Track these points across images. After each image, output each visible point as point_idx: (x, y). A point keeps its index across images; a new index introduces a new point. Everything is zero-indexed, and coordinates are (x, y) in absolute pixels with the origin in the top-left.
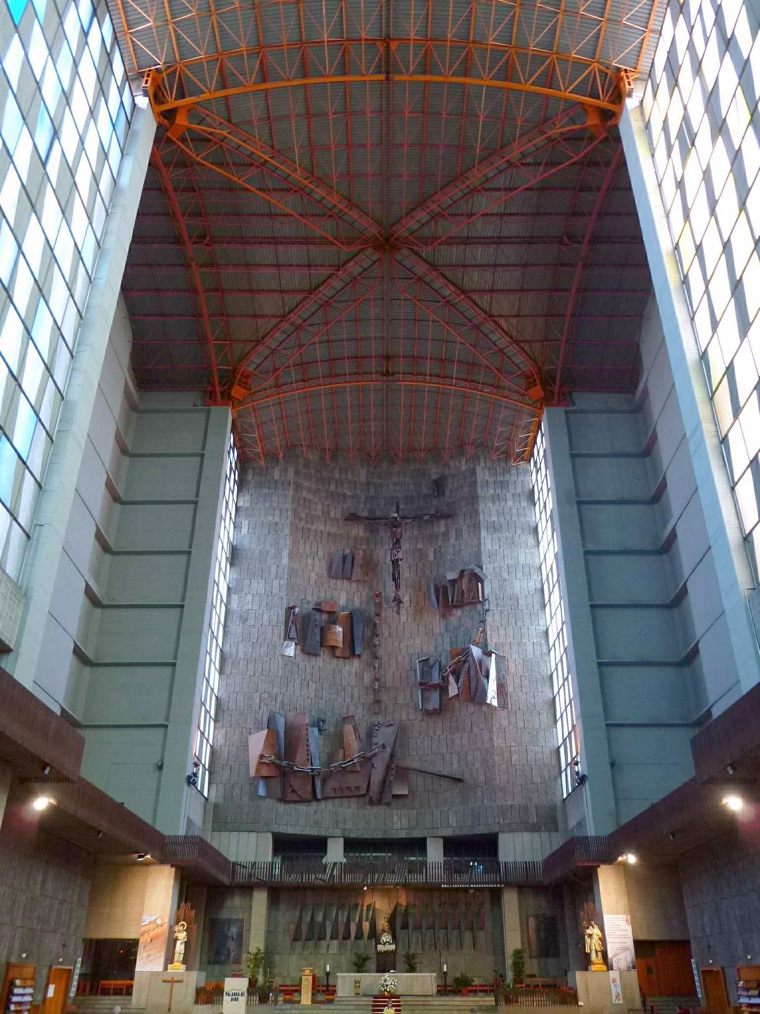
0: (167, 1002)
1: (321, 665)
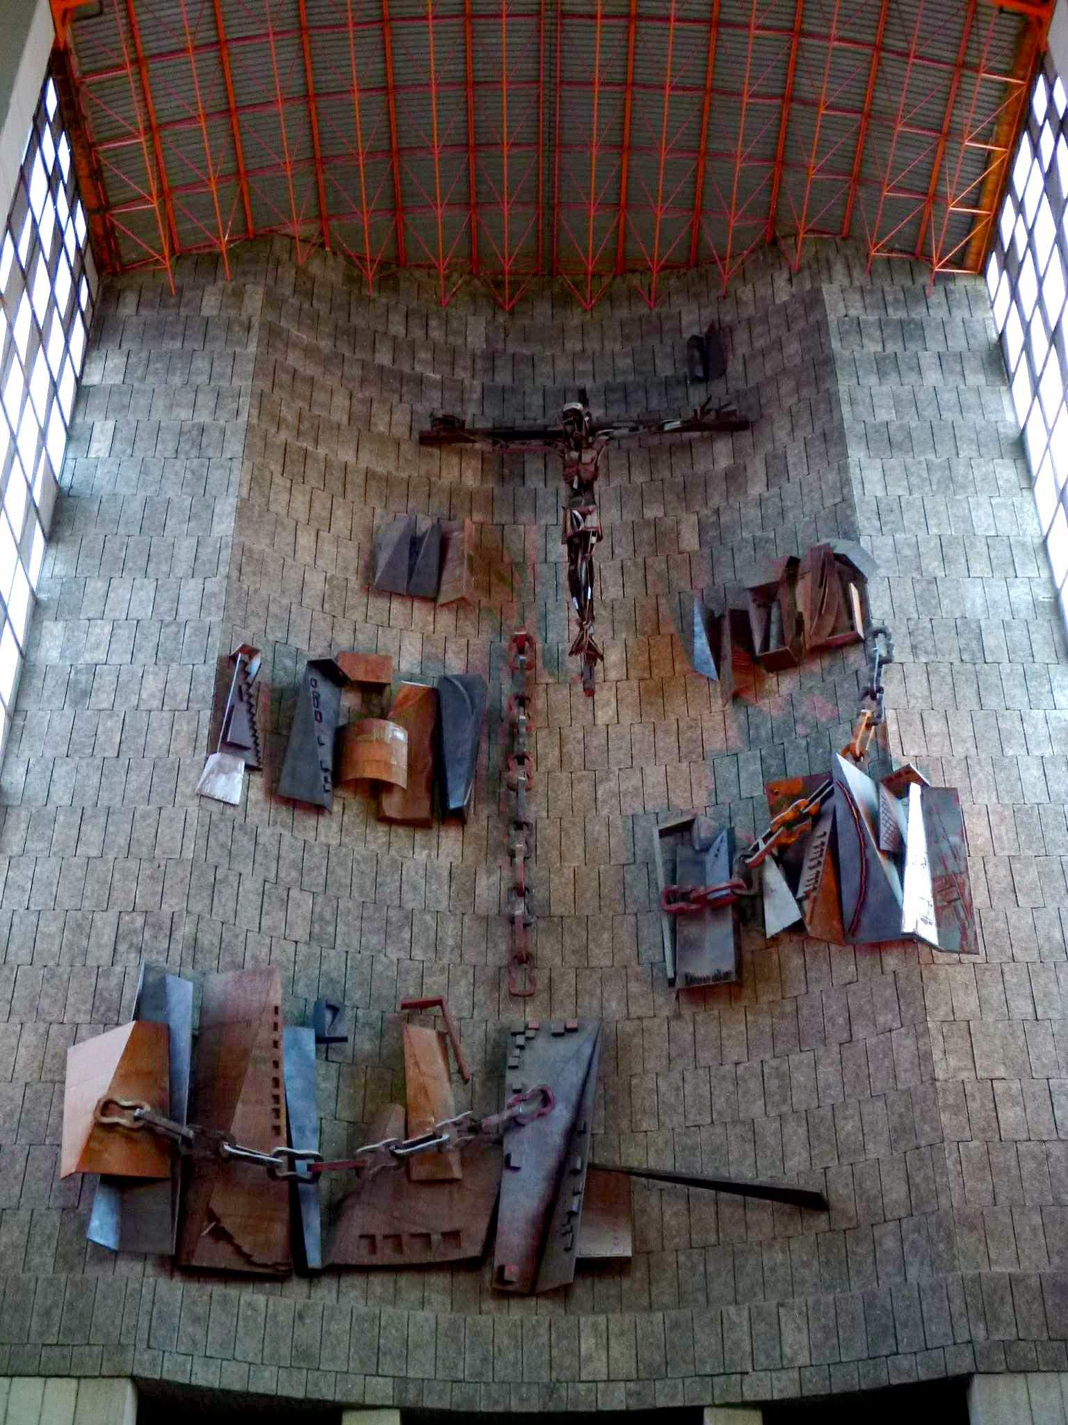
1: (334, 842)
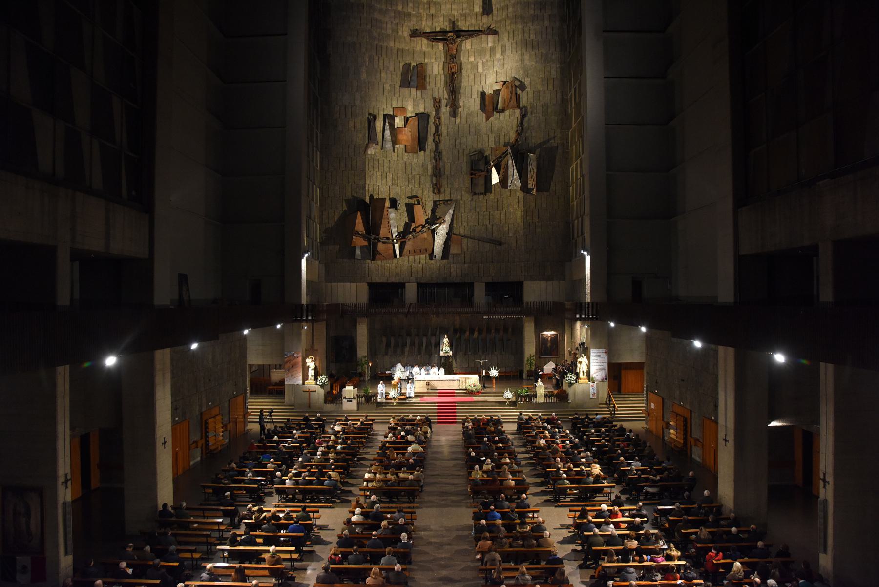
0: (308, 402)
1: (396, 159)
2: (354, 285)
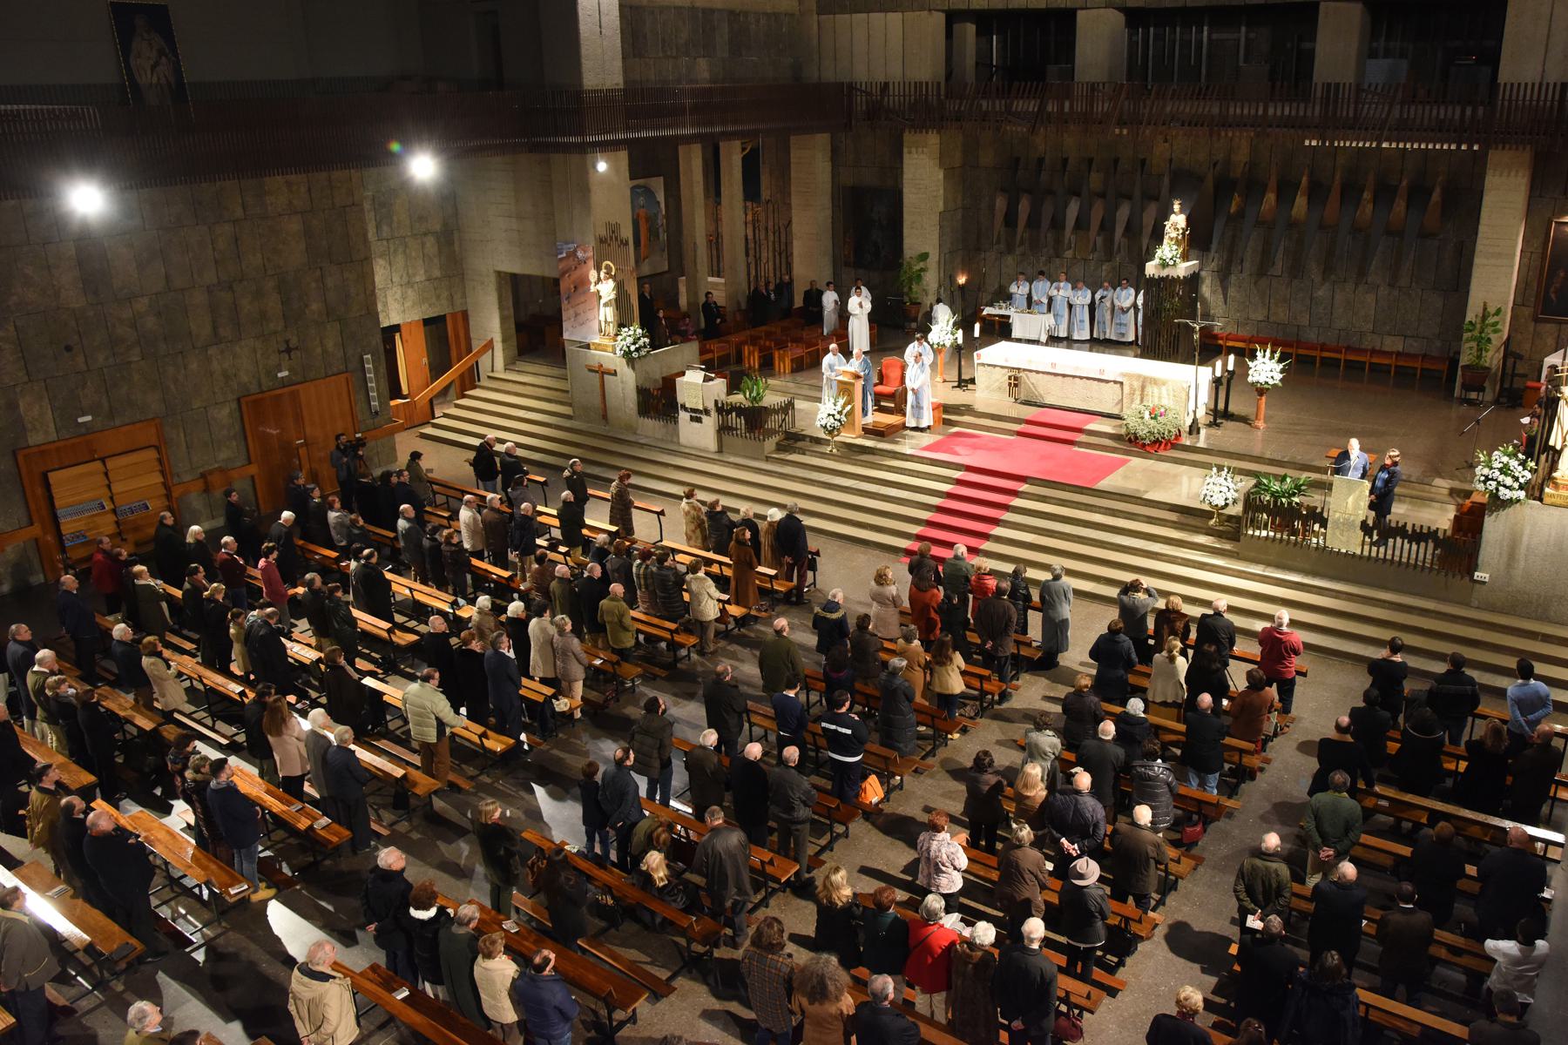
2: (895, 18)
